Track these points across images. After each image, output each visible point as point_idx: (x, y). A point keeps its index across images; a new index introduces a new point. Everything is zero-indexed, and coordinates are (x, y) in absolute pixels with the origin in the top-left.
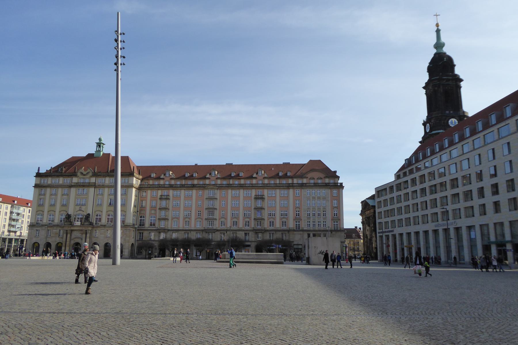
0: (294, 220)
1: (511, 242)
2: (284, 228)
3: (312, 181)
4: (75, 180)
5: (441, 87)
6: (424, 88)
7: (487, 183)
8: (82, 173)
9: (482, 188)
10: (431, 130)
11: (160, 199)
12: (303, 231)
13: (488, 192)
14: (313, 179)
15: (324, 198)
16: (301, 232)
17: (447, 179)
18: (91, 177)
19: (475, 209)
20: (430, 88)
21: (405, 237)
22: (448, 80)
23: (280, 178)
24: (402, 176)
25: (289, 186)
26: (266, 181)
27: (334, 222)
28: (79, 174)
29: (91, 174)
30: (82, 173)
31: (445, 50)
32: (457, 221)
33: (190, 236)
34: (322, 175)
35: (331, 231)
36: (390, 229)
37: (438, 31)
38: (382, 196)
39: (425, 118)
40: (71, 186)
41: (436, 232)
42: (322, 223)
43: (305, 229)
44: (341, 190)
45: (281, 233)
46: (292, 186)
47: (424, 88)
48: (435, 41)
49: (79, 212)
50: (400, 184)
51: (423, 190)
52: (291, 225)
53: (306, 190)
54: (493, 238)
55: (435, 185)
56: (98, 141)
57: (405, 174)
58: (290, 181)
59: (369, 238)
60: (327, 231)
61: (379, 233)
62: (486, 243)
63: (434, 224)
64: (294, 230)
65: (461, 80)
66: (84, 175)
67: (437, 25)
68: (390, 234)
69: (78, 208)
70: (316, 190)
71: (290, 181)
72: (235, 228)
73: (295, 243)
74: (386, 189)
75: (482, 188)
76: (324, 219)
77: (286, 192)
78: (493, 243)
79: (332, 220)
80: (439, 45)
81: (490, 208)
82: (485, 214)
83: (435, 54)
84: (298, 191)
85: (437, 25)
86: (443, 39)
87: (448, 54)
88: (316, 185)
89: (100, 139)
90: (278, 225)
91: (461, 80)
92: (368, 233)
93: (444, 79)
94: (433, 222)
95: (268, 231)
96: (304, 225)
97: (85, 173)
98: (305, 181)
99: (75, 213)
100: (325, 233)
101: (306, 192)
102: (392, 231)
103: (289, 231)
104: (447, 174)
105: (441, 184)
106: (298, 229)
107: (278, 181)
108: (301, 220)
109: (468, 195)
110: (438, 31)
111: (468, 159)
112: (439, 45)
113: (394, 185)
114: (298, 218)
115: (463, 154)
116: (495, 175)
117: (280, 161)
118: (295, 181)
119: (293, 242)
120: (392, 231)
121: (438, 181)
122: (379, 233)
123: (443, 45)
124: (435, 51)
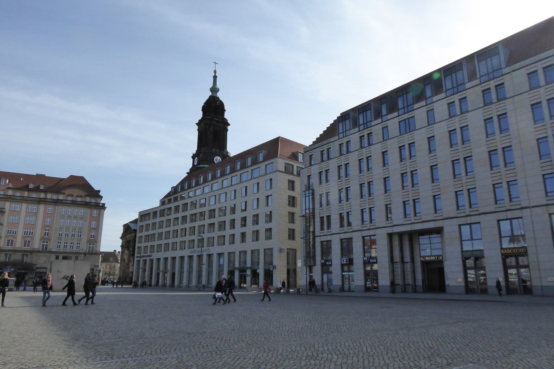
0: (41, 239)
1: (251, 268)
2: (27, 248)
3: (70, 198)
5: (212, 127)
6: (197, 124)
7: (238, 216)
9: (234, 220)
10: (198, 164)
12: (51, 252)
13: (238, 223)
14: (72, 196)
15: (82, 218)
16: (48, 254)
17: (206, 209)
19: (226, 238)
20: (203, 125)
21: (162, 262)
22: (218, 122)
23: (30, 190)
24: (166, 202)
25: (39, 201)
26: (10, 193)
27: (90, 244)
31: (219, 95)
32: (210, 248)
34: (83, 193)
35: (85, 254)
36: (149, 254)
37: (215, 77)
38: (145, 220)
39: (195, 152)
41: (191, 257)
42: (75, 245)
43: (53, 250)
44: (102, 211)
45: (21, 254)
46: (44, 201)
47: (197, 124)
48: (211, 85)
50: (164, 210)
51: (184, 218)
52: (36, 244)
53: (60, 207)
54: (237, 265)
55: (196, 214)
57: (170, 201)
58: (42, 195)
59: (126, 262)
60: (80, 253)
61: (137, 257)
62: (231, 269)
63: (190, 250)
64: (39, 252)
65: (229, 125)
67: (215, 72)
68: (148, 259)
70: (73, 208)
71: (42, 195)
73: (38, 266)
74: (149, 214)
75: (234, 220)
76: (78, 240)
77: (35, 207)
78: (237, 269)
79: (88, 242)
80: (214, 90)
81: (238, 238)
82: (233, 243)
83: (210, 97)
84: (50, 208)
85: (215, 72)
86: (218, 85)
87: (221, 99)
88: (74, 203)
90: (18, 244)
91: (229, 125)
92: (126, 257)
93: (215, 120)
94: (189, 248)
95: (4, 251)
96: (52, 246)
98: (61, 197)
100: (77, 255)
101: (63, 210)
102: (150, 256)
103: (32, 252)
104: (207, 205)
105: (201, 213)
106: (45, 251)
107: (26, 194)
108: (50, 240)
109: (222, 225)
110: (215, 77)
111: (226, 193)
112: (214, 90)
113: (158, 210)
114: (45, 238)
115: (223, 188)
116: (245, 210)
117: (33, 171)
118: (49, 196)
119: (36, 265)
120: (150, 256)
121: (198, 210)
122: (137, 257)
123: (218, 90)
124: (210, 94)
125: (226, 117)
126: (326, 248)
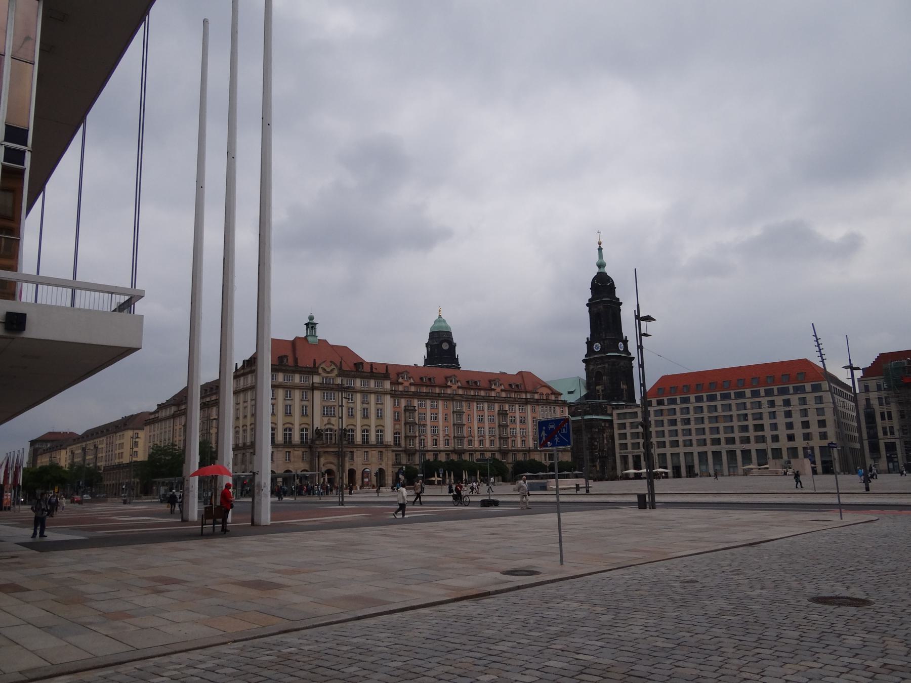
4: (317, 379)
6: (587, 305)
8: (324, 370)
10: (603, 350)
11: (405, 410)
18: (337, 376)
28: (320, 371)
29: (336, 372)
30: (324, 370)
33: (427, 457)
34: (550, 392)
37: (600, 249)
40: (313, 388)
49: (328, 426)
56: (308, 321)
66: (328, 373)
67: (600, 244)
69: (326, 419)
71: (524, 396)
72: (481, 448)
80: (601, 265)
85: (600, 244)
86: (605, 259)
89: (311, 318)
95: (512, 451)
97: (328, 369)
98: (536, 396)
99: (323, 428)
103: (529, 451)
110: (600, 249)
112: (601, 265)
117: (497, 370)
124: (597, 270)
125: (617, 296)
126: (891, 447)
